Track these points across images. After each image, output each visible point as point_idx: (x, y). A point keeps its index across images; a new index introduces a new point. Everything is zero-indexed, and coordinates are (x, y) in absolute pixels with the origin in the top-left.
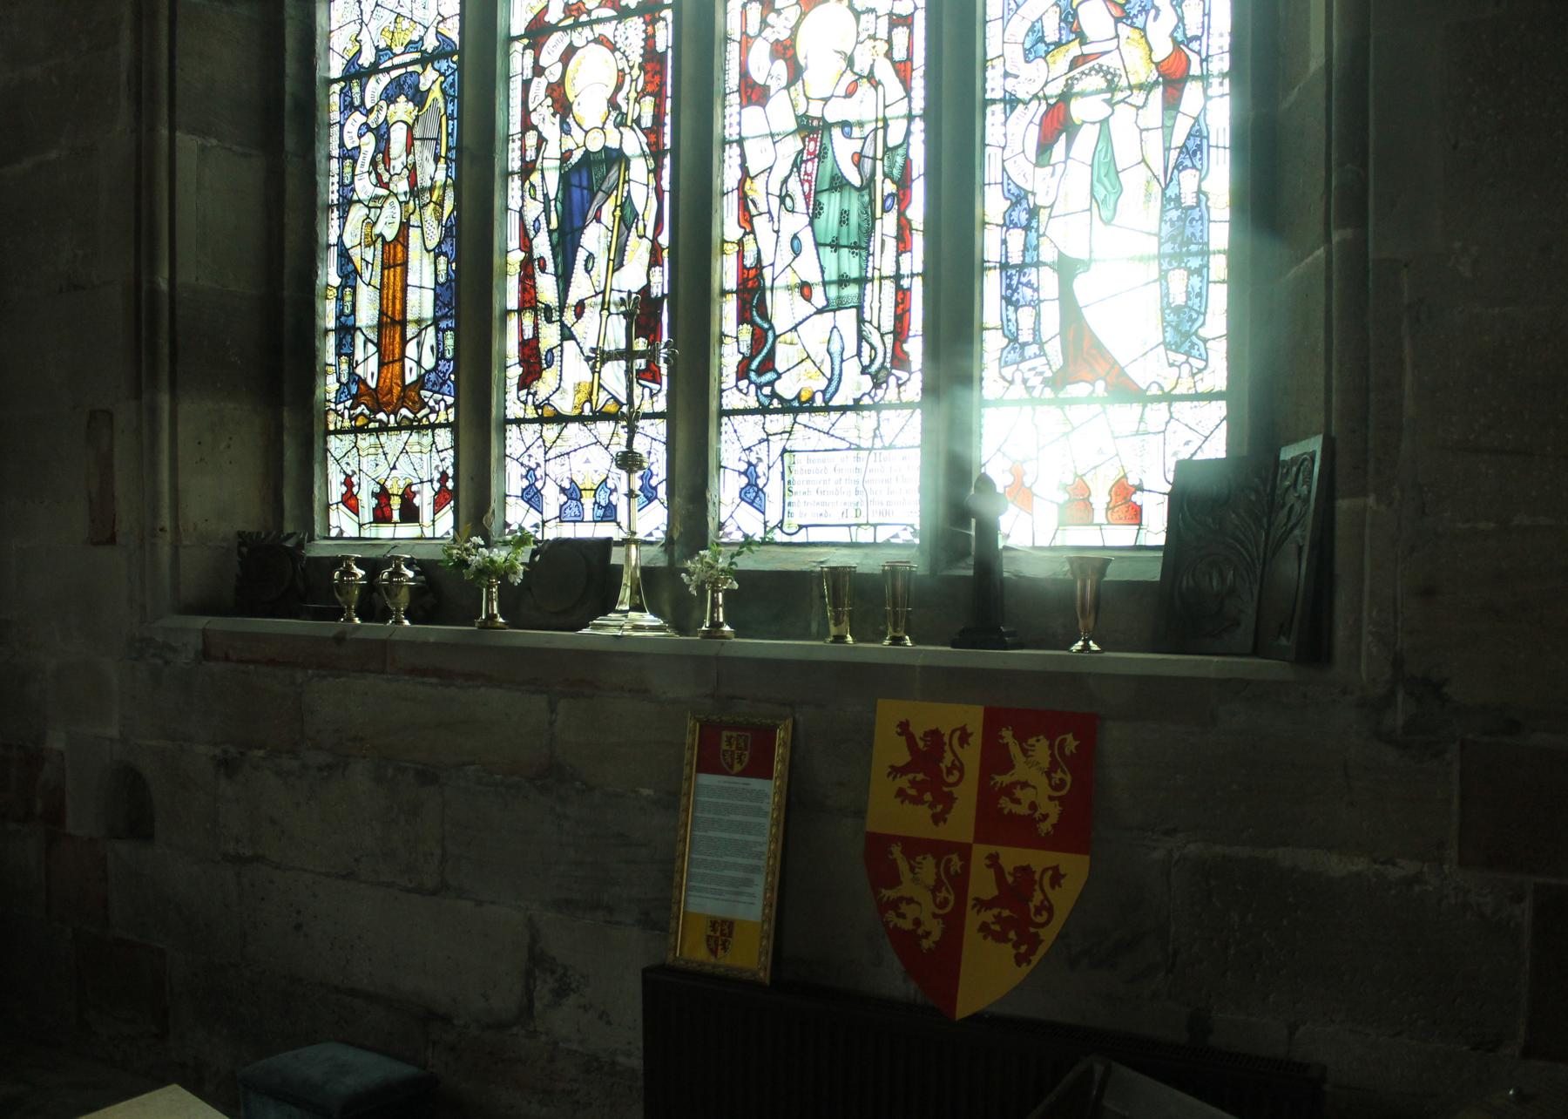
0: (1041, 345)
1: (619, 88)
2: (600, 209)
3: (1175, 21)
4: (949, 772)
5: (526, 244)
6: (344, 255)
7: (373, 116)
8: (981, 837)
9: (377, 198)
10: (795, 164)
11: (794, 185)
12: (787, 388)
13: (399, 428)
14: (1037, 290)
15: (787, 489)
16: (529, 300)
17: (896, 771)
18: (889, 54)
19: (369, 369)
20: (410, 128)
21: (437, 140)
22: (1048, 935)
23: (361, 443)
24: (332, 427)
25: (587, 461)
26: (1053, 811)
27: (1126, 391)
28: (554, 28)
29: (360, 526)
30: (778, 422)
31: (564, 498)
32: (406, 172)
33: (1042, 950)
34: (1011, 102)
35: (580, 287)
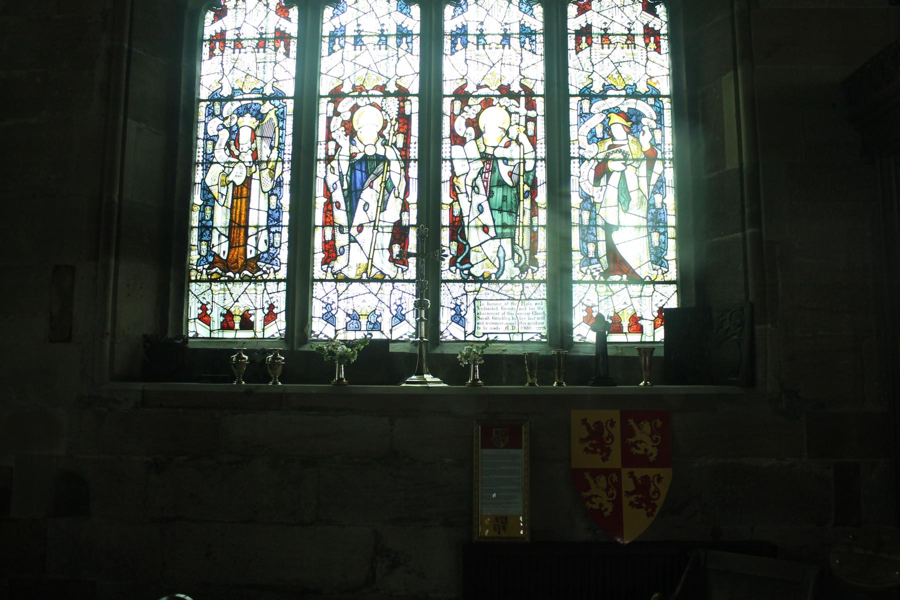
0: (599, 259)
1: (384, 128)
2: (372, 182)
3: (651, 137)
4: (607, 439)
5: (328, 193)
6: (206, 189)
8: (624, 465)
9: (229, 162)
10: (479, 173)
11: (479, 182)
12: (477, 271)
13: (242, 280)
15: (476, 317)
16: (329, 221)
17: (582, 440)
18: (526, 132)
19: (222, 248)
20: (254, 131)
22: (660, 503)
23: (213, 287)
24: (193, 278)
25: (364, 301)
26: (654, 452)
27: (634, 279)
28: (347, 95)
29: (211, 331)
30: (470, 287)
31: (348, 319)
33: (658, 510)
34: (582, 159)
35: (360, 217)
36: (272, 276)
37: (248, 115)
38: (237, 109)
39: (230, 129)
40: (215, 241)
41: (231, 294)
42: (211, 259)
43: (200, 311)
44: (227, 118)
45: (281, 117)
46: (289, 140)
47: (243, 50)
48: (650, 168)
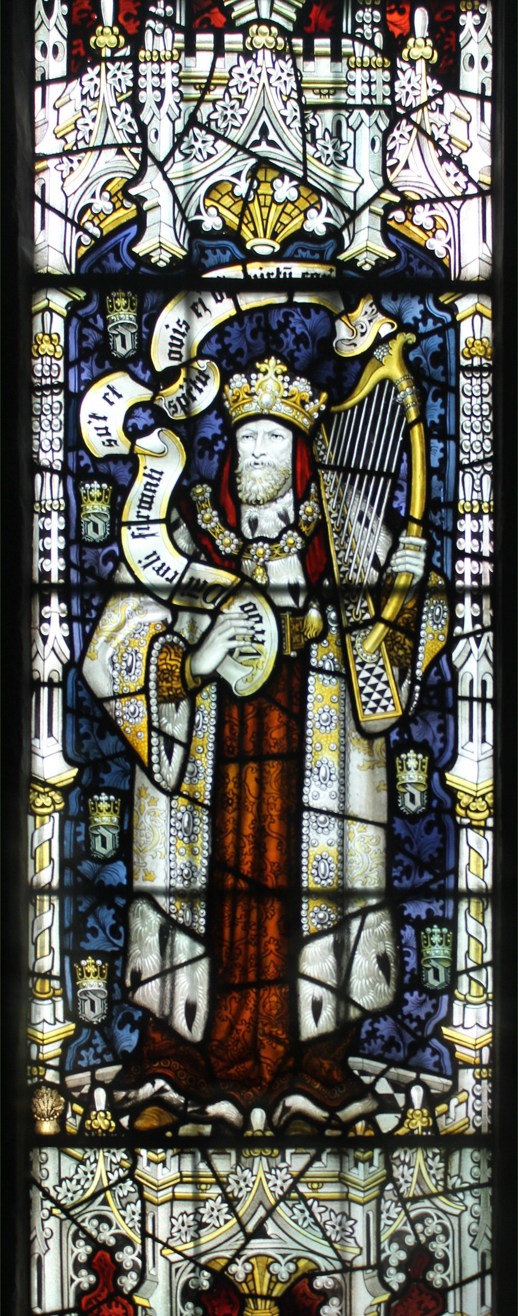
6: (89, 716)
7: (175, 390)
9: (196, 589)
13: (282, 1137)
20: (303, 441)
21: (400, 481)
24: (47, 1127)
32: (293, 539)
36: (418, 1122)
37: (272, 365)
38: (220, 331)
39: (188, 430)
40: (147, 959)
41: (231, 1202)
42: (129, 1039)
43: (86, 1279)
44: (170, 376)
45: (434, 374)
46: (475, 489)
47: (233, 40)
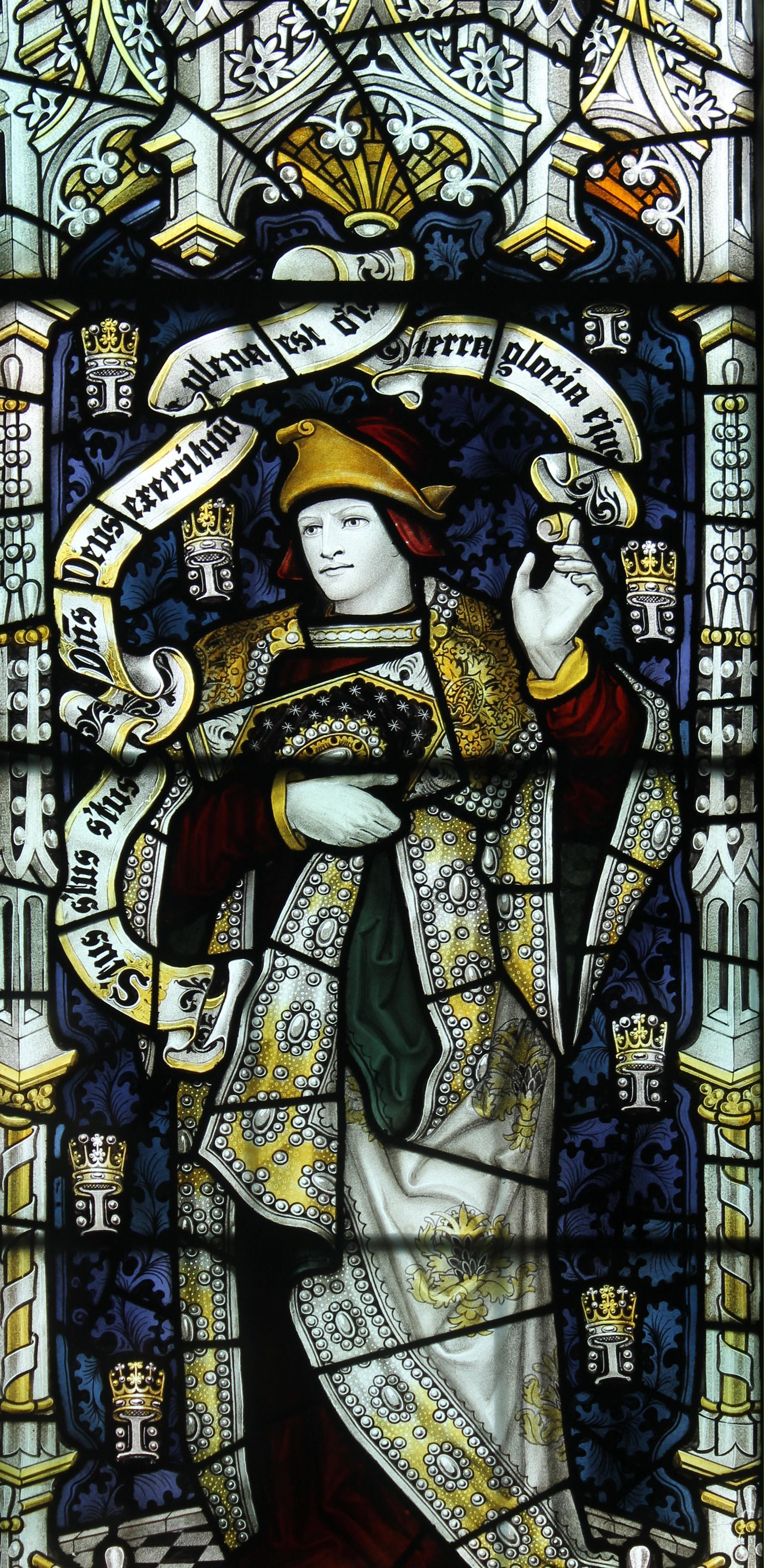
14: (173, 1313)
48: (583, 839)
